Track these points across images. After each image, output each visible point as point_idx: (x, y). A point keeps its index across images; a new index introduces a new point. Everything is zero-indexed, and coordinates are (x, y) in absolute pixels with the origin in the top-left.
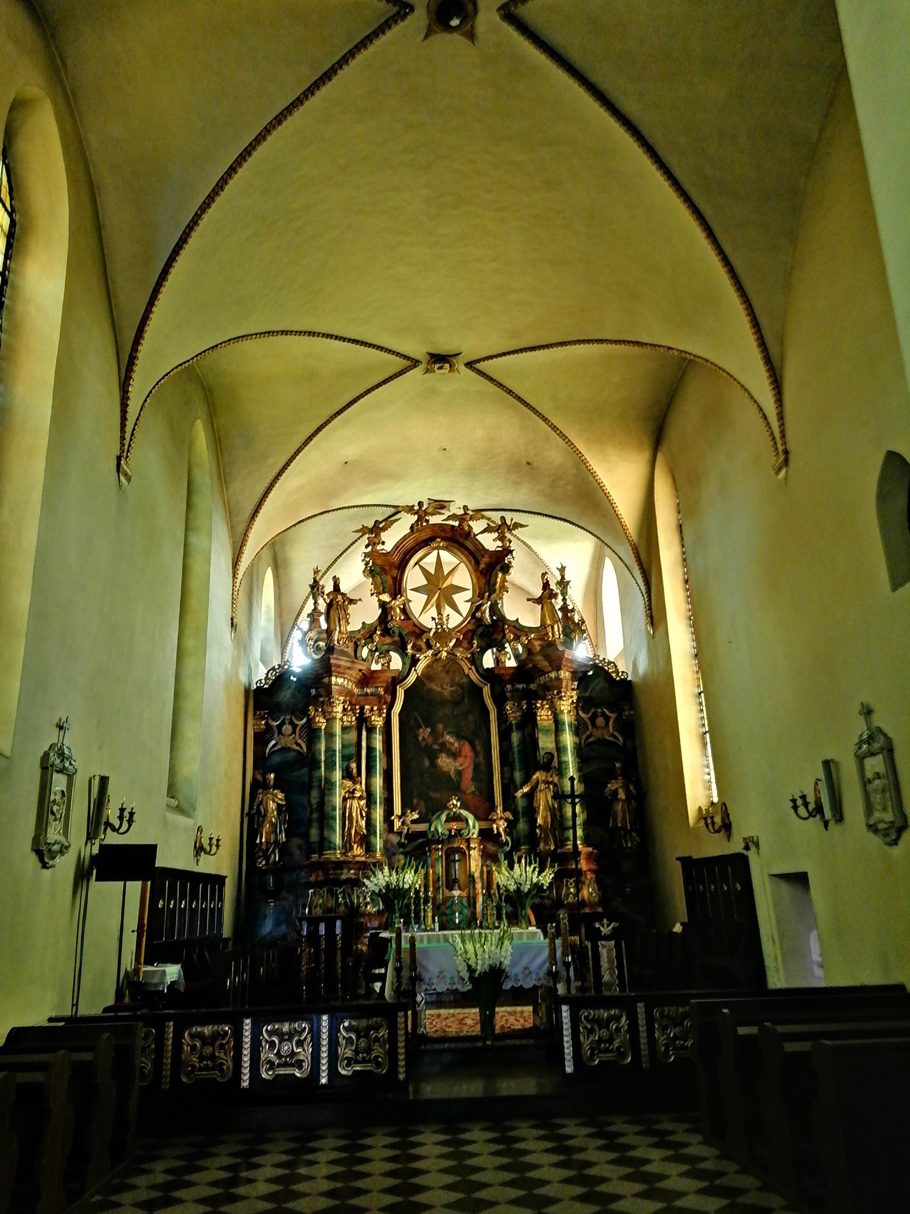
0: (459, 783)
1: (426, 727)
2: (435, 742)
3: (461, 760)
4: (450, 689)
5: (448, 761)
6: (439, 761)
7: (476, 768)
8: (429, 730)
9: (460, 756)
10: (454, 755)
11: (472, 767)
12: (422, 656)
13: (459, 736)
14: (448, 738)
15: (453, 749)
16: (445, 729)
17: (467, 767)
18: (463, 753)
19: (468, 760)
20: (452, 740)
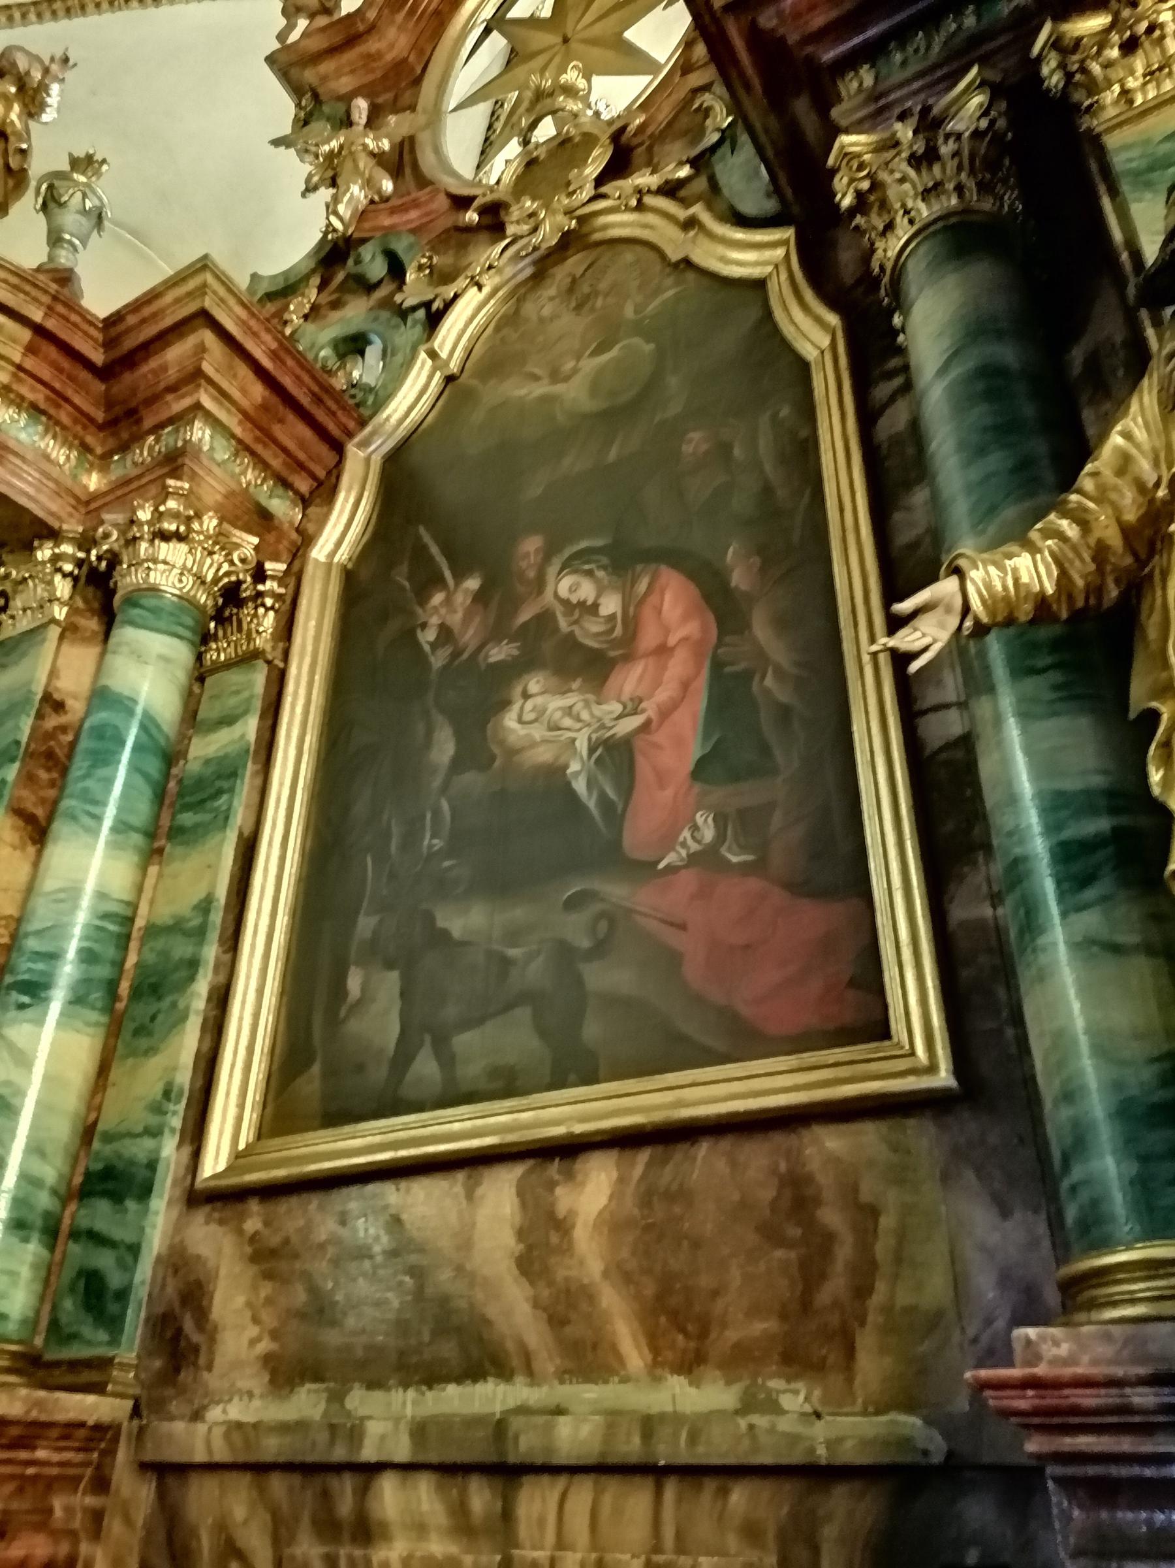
0: (614, 814)
1: (460, 575)
2: (496, 634)
3: (629, 679)
4: (590, 364)
5: (554, 704)
6: (510, 720)
7: (729, 693)
8: (473, 584)
9: (629, 658)
10: (590, 666)
11: (700, 701)
12: (461, 282)
13: (623, 560)
14: (571, 586)
15: (590, 632)
16: (548, 554)
17: (665, 713)
18: (649, 638)
19: (678, 666)
20: (587, 591)
